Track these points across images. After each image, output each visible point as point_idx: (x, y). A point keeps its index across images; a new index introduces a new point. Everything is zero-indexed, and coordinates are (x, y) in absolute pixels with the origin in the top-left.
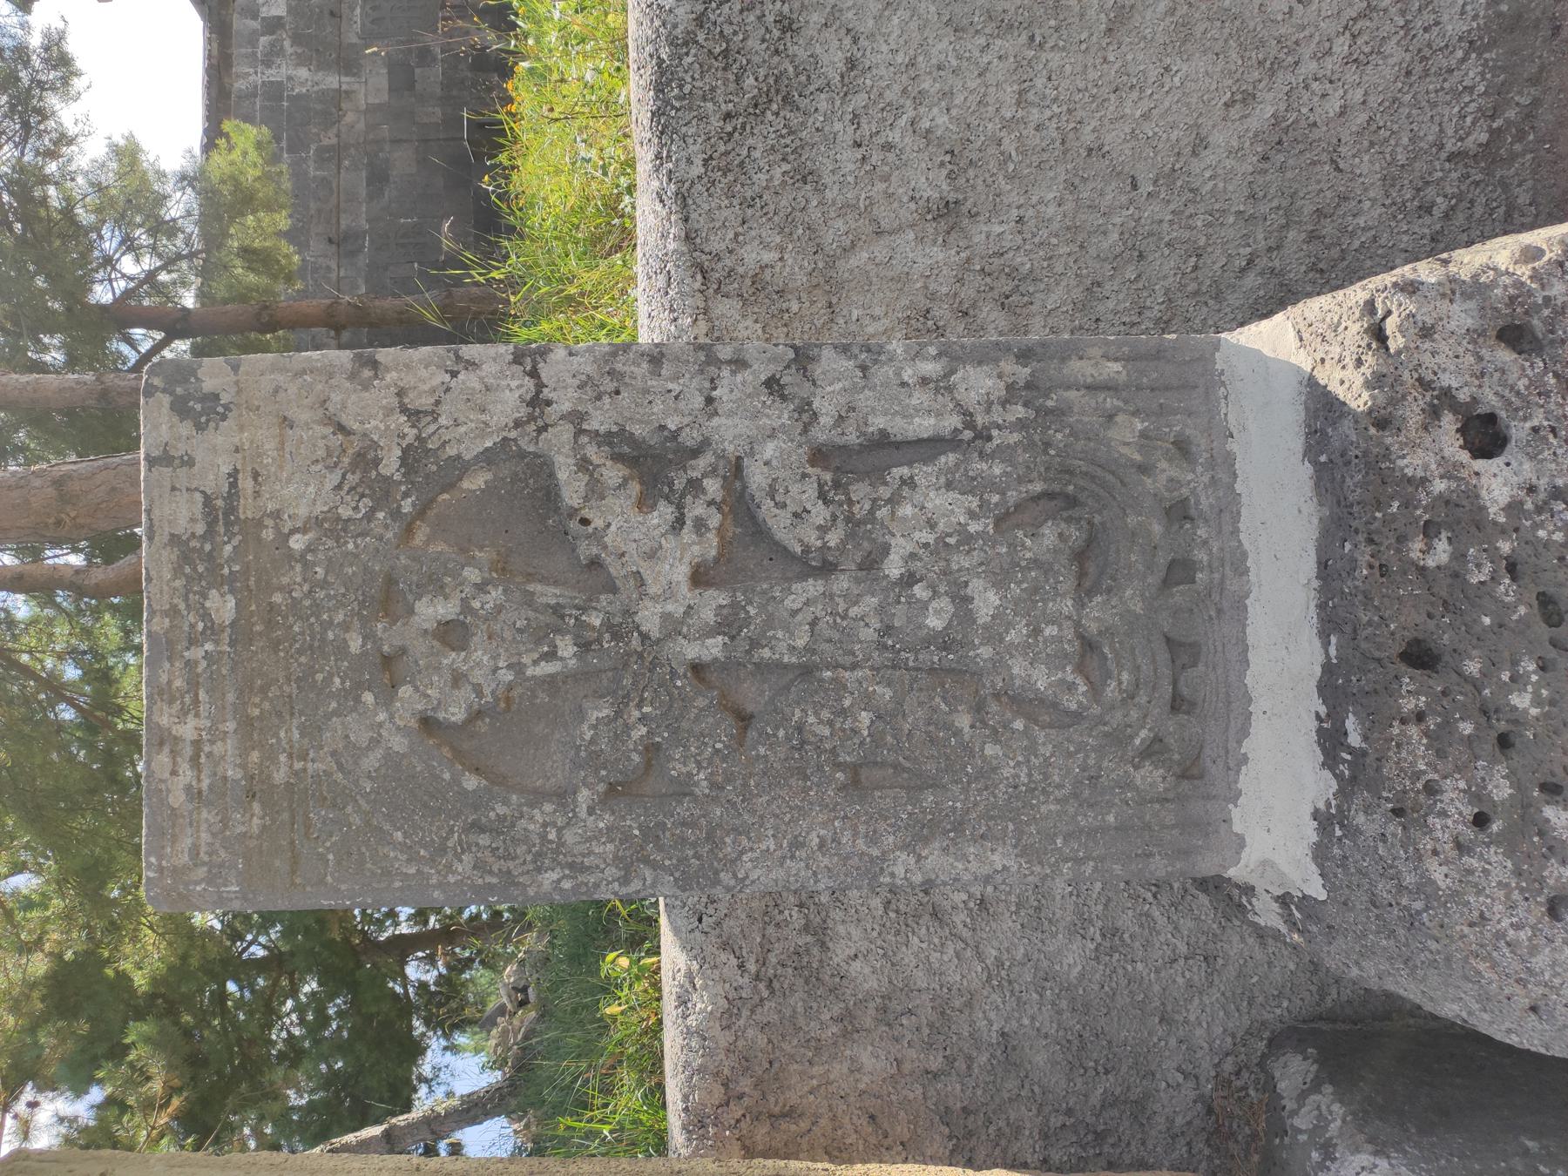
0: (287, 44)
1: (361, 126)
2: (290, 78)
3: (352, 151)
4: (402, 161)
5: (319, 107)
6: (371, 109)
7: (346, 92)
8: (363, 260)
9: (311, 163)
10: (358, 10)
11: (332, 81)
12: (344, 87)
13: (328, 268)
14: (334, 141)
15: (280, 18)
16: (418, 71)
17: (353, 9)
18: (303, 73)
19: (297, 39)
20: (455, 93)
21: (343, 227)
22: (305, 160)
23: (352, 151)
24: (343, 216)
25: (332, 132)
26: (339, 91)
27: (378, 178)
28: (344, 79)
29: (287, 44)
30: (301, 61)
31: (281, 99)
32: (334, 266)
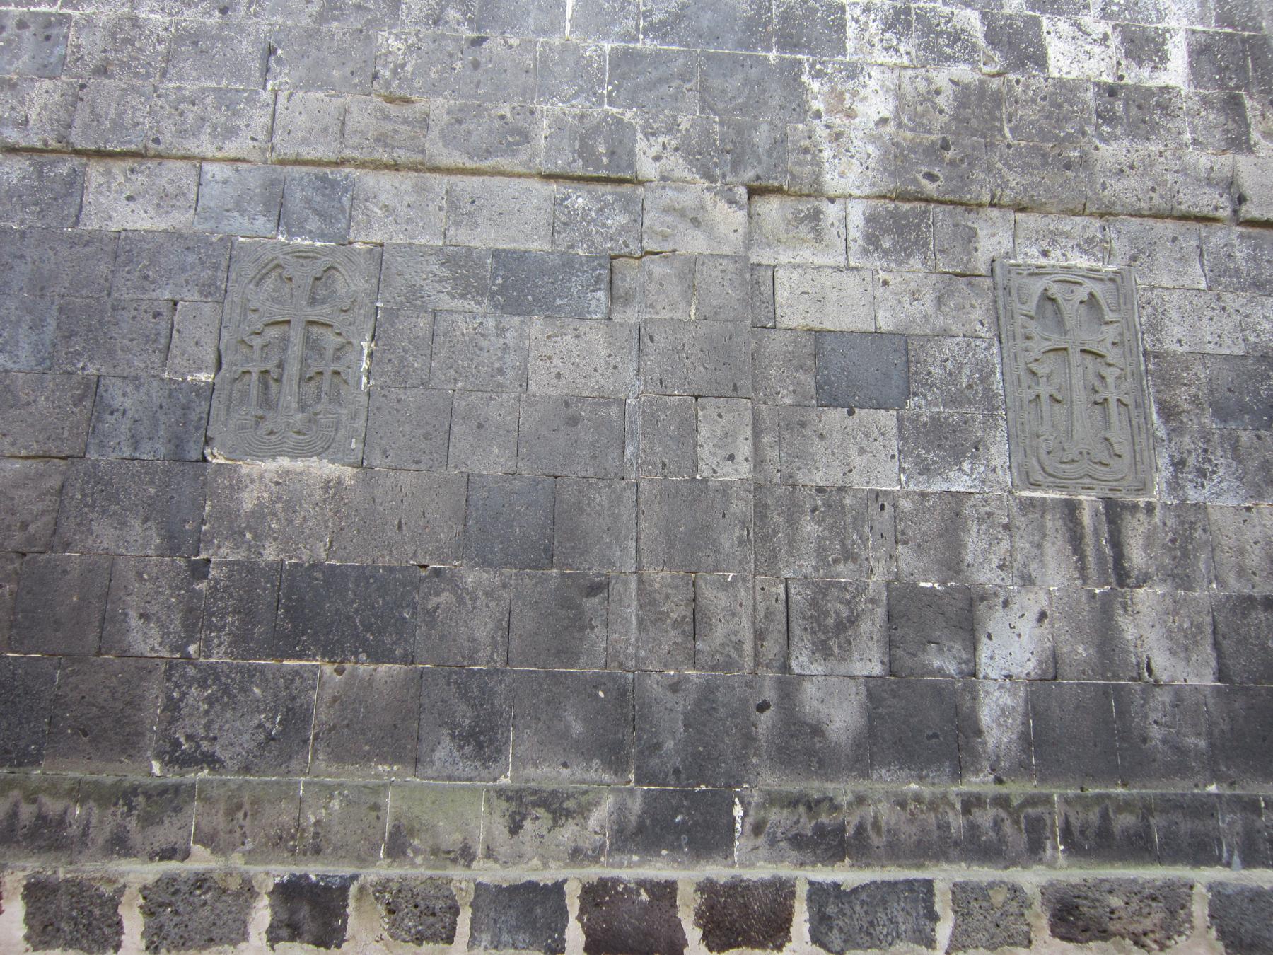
0: (962, 71)
1: (695, 243)
2: (853, 72)
3: (618, 219)
4: (572, 356)
5: (762, 136)
6: (755, 283)
7: (815, 216)
8: (251, 227)
9: (580, 105)
10: (1081, 261)
11: (850, 175)
12: (831, 212)
13: (231, 132)
14: (647, 168)
15: (1041, 61)
16: (887, 419)
17: (1088, 245)
18: (875, 104)
19: (979, 104)
20: (809, 528)
21: (370, 180)
22: (591, 91)
23: (618, 219)
24: (406, 181)
25: (677, 165)
26: (817, 192)
27: (518, 285)
28: (857, 213)
29: (962, 71)
30: (913, 108)
31: (788, 42)
32: (233, 148)
